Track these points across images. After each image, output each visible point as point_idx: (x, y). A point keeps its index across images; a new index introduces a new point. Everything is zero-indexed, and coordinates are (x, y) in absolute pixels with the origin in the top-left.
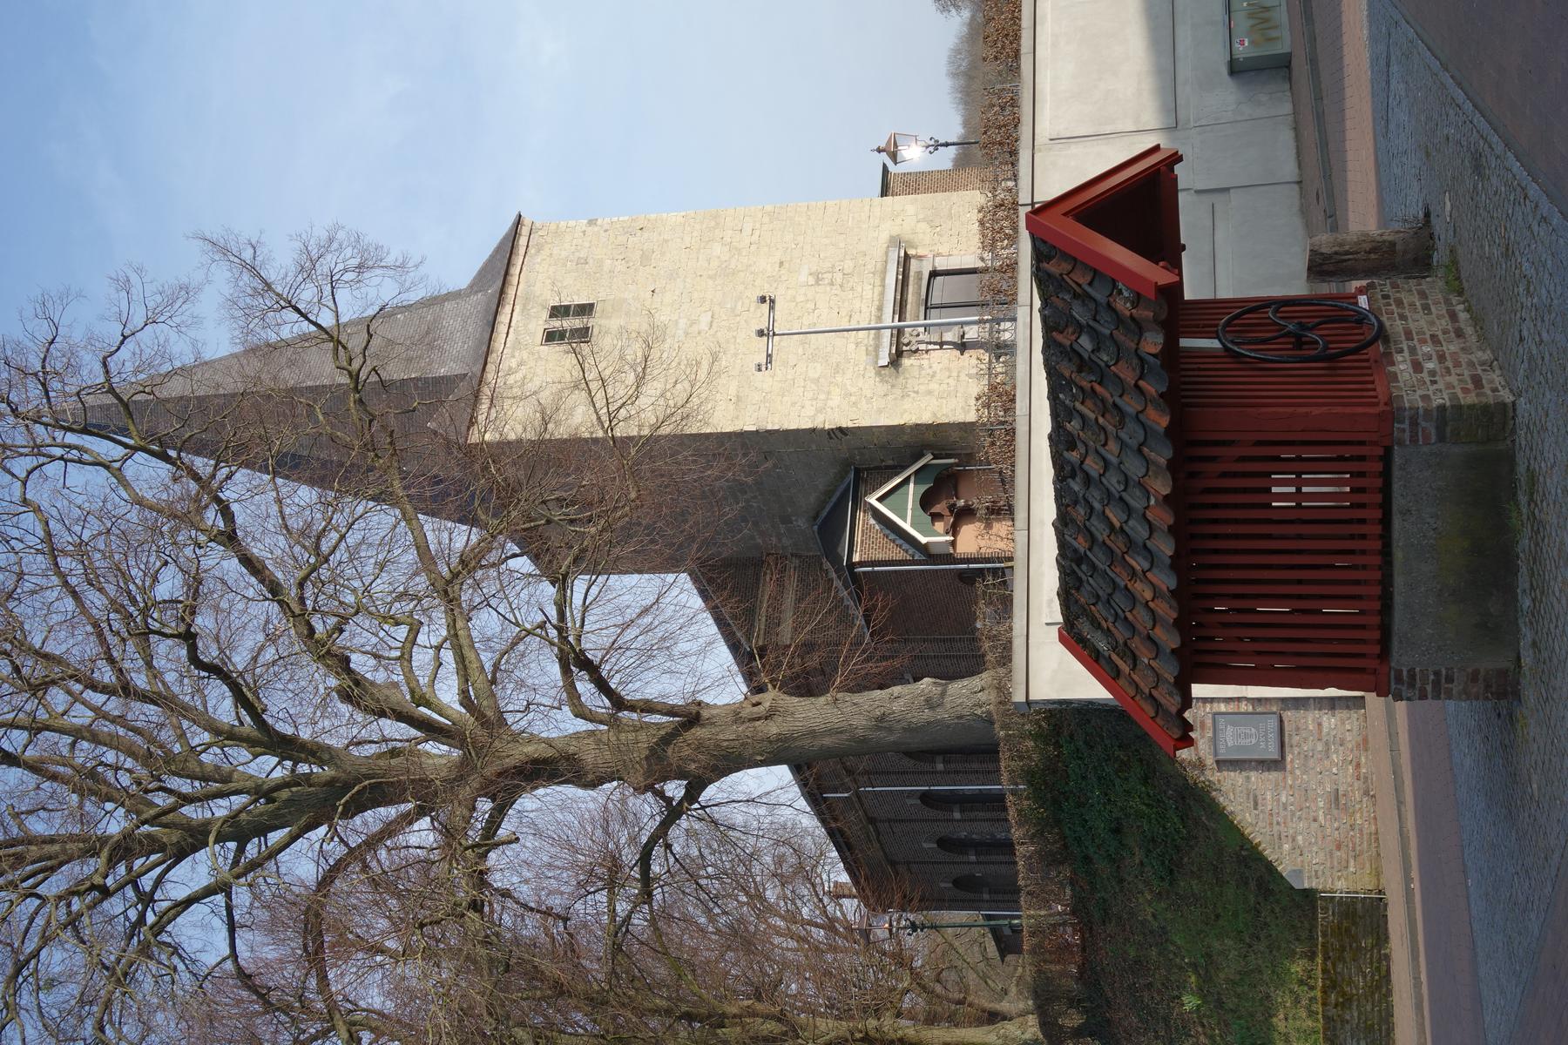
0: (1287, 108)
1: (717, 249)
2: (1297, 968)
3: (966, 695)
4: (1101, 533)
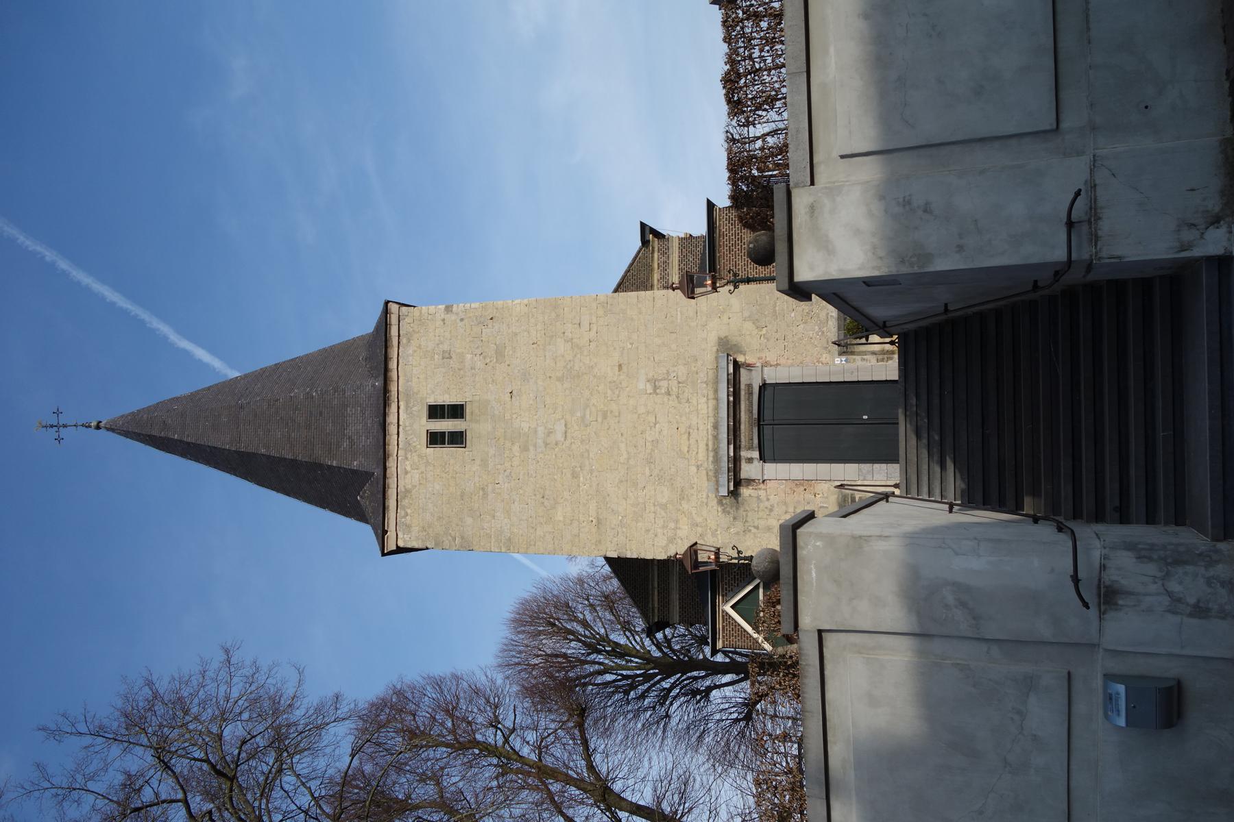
1: (561, 347)
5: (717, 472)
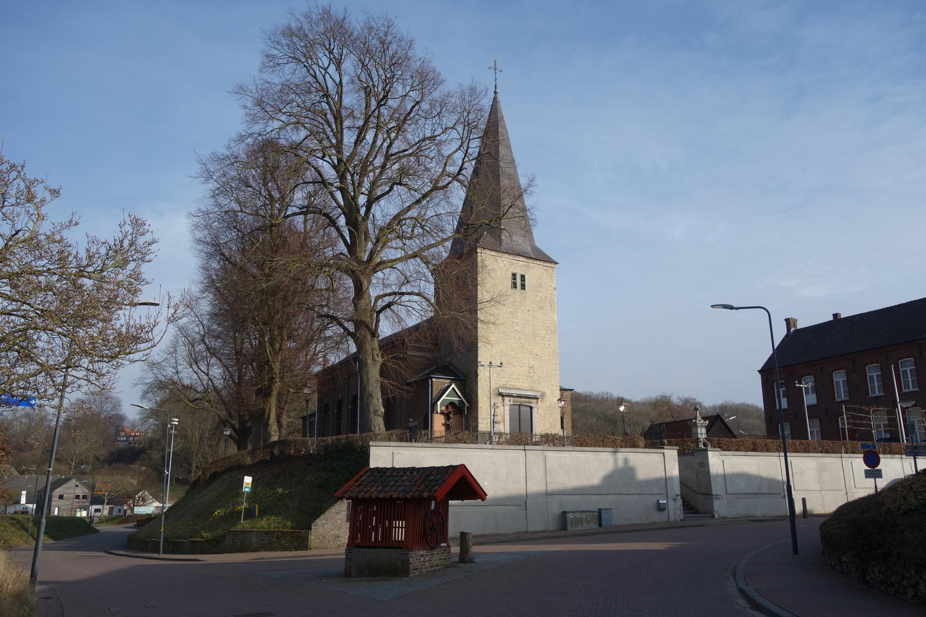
0: (551, 529)
1: (543, 333)
2: (289, 524)
3: (379, 423)
4: (388, 480)
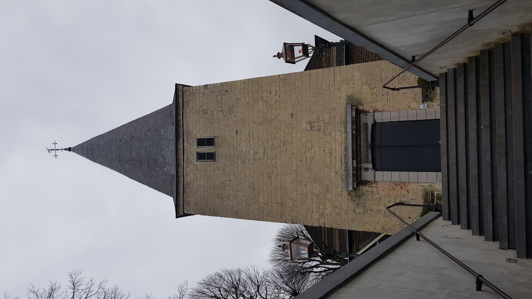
5: (347, 176)
